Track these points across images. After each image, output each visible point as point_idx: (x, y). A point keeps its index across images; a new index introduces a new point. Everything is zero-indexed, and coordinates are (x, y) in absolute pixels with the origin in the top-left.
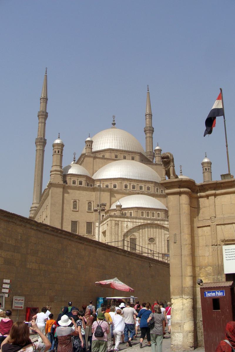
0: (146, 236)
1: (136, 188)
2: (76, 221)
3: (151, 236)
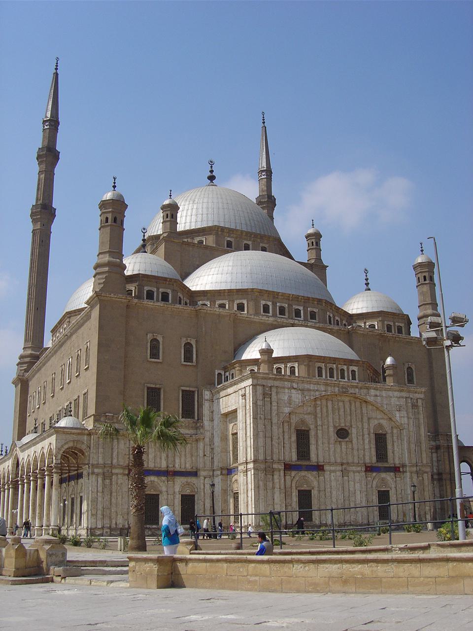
1: (287, 314)
2: (158, 386)
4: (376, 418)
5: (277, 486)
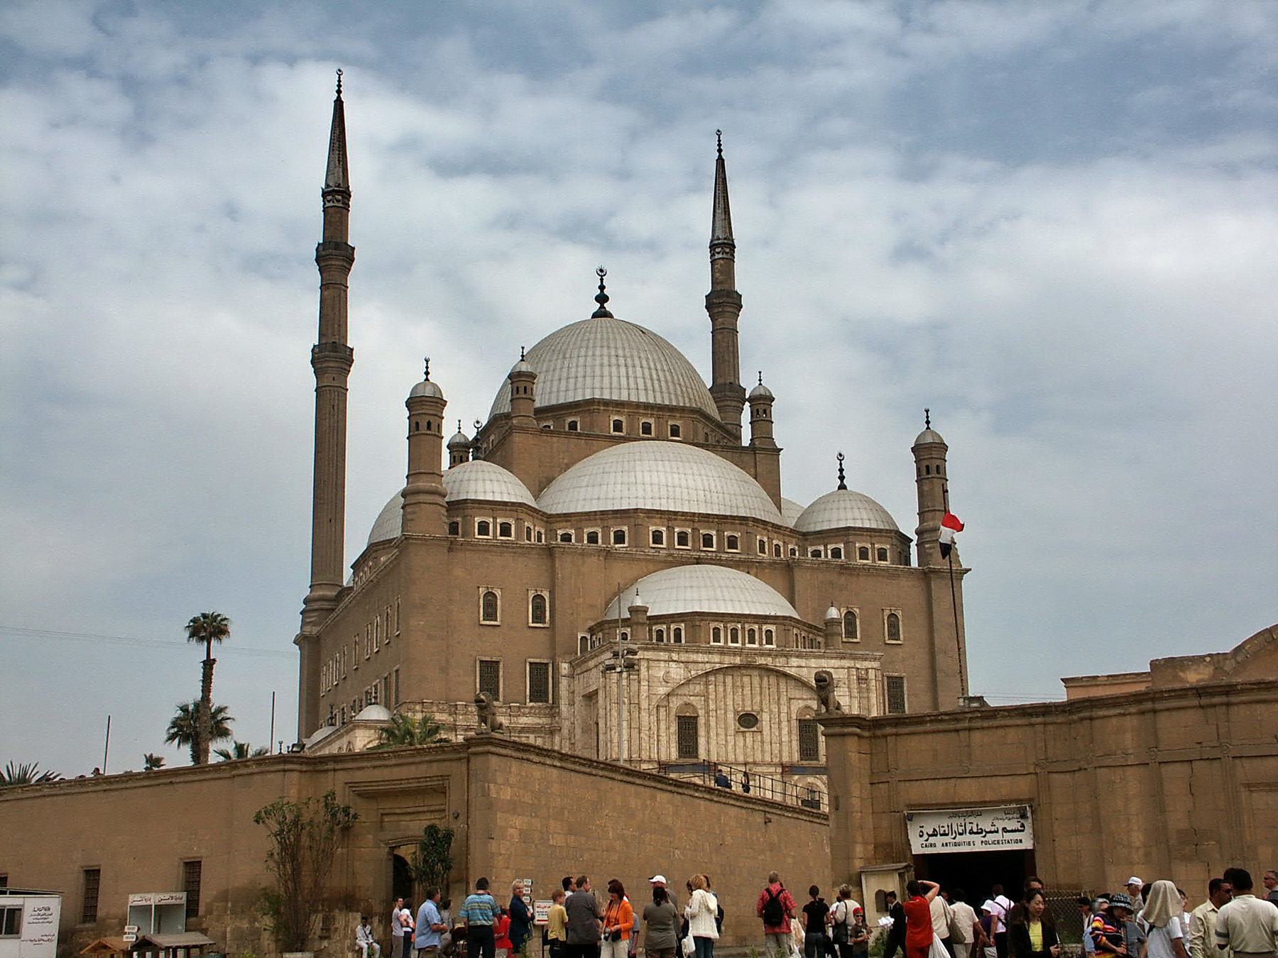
1: (690, 543)
3: (744, 706)
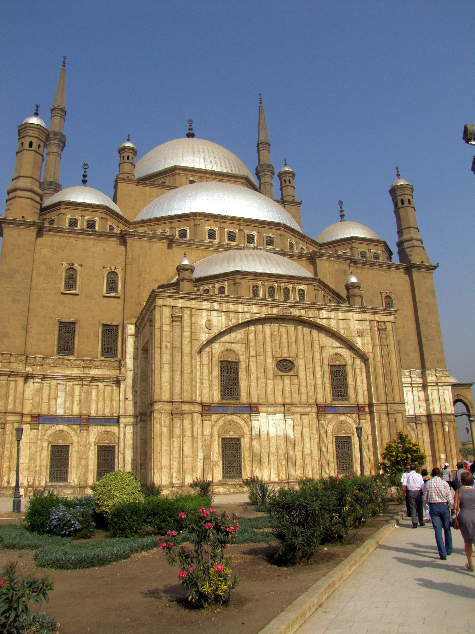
0: (269, 354)
1: (237, 239)
2: (72, 320)
3: (281, 353)
4: (332, 347)
5: (188, 433)
